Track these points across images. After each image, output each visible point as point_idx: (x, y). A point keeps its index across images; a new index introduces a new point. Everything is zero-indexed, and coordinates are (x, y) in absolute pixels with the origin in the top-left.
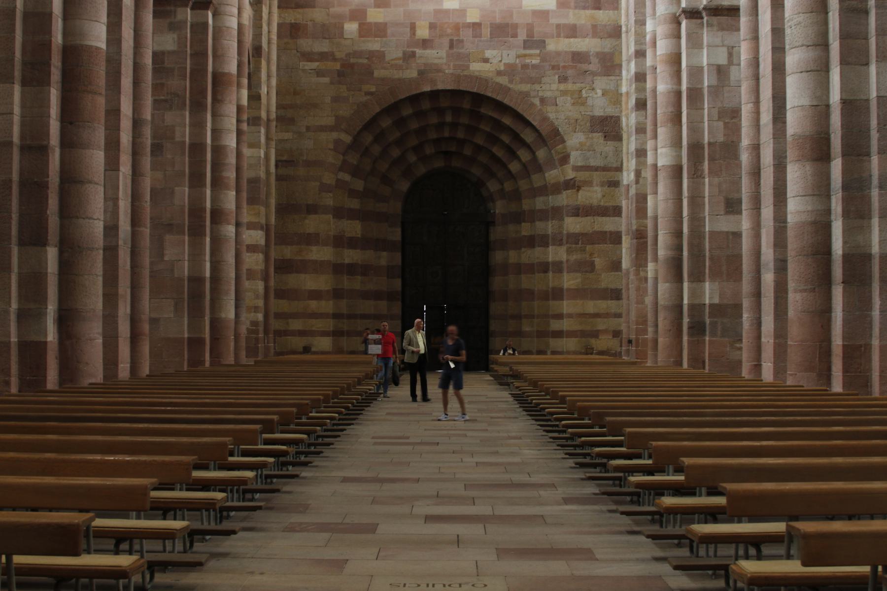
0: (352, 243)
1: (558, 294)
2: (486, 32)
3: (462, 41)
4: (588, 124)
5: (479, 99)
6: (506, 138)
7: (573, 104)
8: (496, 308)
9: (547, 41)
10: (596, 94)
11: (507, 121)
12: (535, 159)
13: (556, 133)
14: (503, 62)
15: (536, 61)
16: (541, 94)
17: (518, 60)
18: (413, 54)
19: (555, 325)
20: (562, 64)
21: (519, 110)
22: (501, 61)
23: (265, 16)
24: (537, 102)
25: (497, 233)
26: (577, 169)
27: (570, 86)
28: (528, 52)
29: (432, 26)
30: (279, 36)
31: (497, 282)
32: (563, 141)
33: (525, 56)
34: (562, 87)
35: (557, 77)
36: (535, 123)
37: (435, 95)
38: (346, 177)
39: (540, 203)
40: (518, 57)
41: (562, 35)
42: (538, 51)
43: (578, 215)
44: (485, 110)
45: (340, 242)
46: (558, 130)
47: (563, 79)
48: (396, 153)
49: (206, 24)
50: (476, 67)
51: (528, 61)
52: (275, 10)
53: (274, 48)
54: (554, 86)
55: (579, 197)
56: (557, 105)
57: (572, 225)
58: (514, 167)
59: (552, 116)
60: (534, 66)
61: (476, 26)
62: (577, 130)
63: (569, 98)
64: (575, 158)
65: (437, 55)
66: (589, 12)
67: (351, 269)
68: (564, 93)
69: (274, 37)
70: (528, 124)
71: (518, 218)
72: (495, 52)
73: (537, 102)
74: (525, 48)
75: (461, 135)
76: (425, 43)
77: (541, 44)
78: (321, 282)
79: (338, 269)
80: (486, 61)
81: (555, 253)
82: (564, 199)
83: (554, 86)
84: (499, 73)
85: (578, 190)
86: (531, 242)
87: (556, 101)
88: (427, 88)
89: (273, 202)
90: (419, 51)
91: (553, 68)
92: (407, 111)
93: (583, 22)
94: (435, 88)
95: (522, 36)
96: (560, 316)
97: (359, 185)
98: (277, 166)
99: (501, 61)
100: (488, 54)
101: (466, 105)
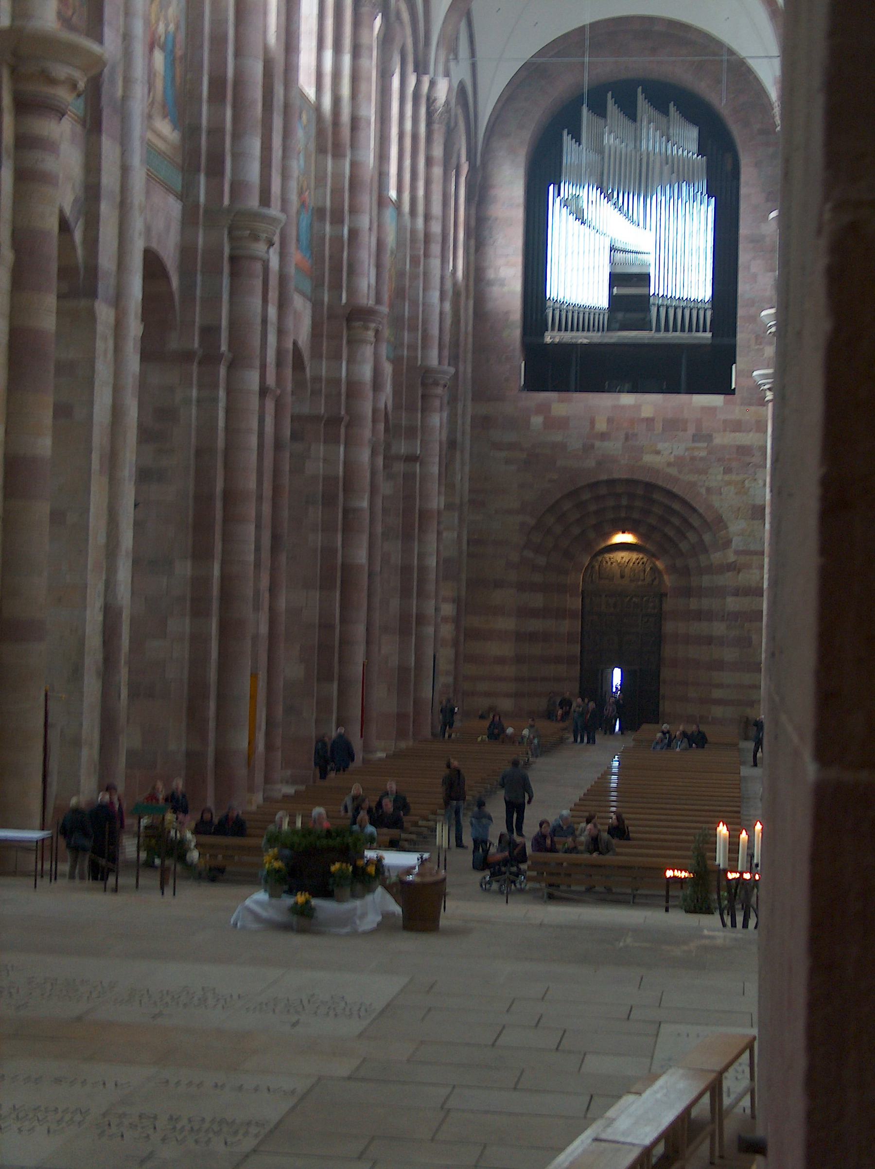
0: (534, 613)
1: (718, 665)
2: (659, 426)
3: (636, 435)
4: (750, 512)
5: (650, 487)
6: (676, 521)
7: (736, 494)
8: (666, 673)
9: (715, 435)
10: (758, 484)
11: (676, 506)
12: (702, 541)
13: (720, 520)
14: (674, 453)
15: (703, 454)
16: (706, 484)
17: (686, 454)
18: (592, 446)
19: (717, 694)
20: (727, 457)
21: (688, 498)
22: (671, 453)
23: (460, 412)
24: (703, 491)
25: (669, 604)
26: (737, 553)
27: (733, 477)
28: (697, 445)
29: (610, 421)
30: (473, 427)
31: (668, 651)
32: (726, 528)
33: (693, 449)
34: (727, 478)
35: (723, 468)
36: (701, 511)
37: (611, 482)
38: (529, 554)
39: (706, 581)
40: (687, 449)
41: (728, 429)
42: (705, 445)
43: (737, 595)
44: (656, 496)
45: (525, 612)
46: (722, 517)
47: (728, 471)
48: (576, 531)
49: (414, 475)
50: (648, 459)
51: (696, 453)
52: (469, 403)
53: (468, 437)
54: (719, 477)
55: (740, 578)
56: (721, 494)
57: (732, 603)
58: (684, 546)
59: (717, 504)
60: (702, 459)
61: (650, 421)
62: (739, 517)
63: (733, 488)
64: (737, 543)
65: (614, 447)
66: (753, 409)
67: (533, 637)
68: (729, 483)
69: (468, 429)
70: (694, 510)
71: (687, 592)
72: (666, 445)
73: (703, 491)
74: (694, 441)
75: (636, 515)
76: (603, 436)
77: (709, 438)
78: (506, 649)
79: (520, 637)
80: (658, 453)
81: (719, 628)
82: (727, 580)
83: (719, 477)
84: (669, 464)
85: (739, 573)
86: (699, 615)
87: (721, 491)
88: (604, 477)
89: (464, 576)
90: (598, 444)
91: (719, 460)
92: (586, 496)
93: (748, 418)
94: (611, 477)
95: (691, 430)
96: (720, 686)
97: (541, 560)
98: (468, 544)
99: (671, 453)
100: (660, 446)
101: (640, 491)
